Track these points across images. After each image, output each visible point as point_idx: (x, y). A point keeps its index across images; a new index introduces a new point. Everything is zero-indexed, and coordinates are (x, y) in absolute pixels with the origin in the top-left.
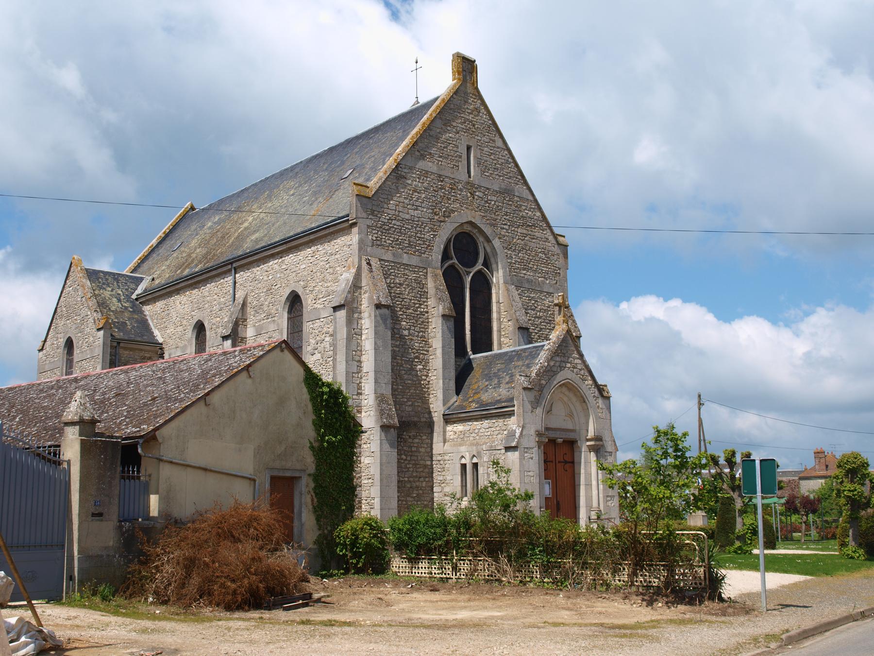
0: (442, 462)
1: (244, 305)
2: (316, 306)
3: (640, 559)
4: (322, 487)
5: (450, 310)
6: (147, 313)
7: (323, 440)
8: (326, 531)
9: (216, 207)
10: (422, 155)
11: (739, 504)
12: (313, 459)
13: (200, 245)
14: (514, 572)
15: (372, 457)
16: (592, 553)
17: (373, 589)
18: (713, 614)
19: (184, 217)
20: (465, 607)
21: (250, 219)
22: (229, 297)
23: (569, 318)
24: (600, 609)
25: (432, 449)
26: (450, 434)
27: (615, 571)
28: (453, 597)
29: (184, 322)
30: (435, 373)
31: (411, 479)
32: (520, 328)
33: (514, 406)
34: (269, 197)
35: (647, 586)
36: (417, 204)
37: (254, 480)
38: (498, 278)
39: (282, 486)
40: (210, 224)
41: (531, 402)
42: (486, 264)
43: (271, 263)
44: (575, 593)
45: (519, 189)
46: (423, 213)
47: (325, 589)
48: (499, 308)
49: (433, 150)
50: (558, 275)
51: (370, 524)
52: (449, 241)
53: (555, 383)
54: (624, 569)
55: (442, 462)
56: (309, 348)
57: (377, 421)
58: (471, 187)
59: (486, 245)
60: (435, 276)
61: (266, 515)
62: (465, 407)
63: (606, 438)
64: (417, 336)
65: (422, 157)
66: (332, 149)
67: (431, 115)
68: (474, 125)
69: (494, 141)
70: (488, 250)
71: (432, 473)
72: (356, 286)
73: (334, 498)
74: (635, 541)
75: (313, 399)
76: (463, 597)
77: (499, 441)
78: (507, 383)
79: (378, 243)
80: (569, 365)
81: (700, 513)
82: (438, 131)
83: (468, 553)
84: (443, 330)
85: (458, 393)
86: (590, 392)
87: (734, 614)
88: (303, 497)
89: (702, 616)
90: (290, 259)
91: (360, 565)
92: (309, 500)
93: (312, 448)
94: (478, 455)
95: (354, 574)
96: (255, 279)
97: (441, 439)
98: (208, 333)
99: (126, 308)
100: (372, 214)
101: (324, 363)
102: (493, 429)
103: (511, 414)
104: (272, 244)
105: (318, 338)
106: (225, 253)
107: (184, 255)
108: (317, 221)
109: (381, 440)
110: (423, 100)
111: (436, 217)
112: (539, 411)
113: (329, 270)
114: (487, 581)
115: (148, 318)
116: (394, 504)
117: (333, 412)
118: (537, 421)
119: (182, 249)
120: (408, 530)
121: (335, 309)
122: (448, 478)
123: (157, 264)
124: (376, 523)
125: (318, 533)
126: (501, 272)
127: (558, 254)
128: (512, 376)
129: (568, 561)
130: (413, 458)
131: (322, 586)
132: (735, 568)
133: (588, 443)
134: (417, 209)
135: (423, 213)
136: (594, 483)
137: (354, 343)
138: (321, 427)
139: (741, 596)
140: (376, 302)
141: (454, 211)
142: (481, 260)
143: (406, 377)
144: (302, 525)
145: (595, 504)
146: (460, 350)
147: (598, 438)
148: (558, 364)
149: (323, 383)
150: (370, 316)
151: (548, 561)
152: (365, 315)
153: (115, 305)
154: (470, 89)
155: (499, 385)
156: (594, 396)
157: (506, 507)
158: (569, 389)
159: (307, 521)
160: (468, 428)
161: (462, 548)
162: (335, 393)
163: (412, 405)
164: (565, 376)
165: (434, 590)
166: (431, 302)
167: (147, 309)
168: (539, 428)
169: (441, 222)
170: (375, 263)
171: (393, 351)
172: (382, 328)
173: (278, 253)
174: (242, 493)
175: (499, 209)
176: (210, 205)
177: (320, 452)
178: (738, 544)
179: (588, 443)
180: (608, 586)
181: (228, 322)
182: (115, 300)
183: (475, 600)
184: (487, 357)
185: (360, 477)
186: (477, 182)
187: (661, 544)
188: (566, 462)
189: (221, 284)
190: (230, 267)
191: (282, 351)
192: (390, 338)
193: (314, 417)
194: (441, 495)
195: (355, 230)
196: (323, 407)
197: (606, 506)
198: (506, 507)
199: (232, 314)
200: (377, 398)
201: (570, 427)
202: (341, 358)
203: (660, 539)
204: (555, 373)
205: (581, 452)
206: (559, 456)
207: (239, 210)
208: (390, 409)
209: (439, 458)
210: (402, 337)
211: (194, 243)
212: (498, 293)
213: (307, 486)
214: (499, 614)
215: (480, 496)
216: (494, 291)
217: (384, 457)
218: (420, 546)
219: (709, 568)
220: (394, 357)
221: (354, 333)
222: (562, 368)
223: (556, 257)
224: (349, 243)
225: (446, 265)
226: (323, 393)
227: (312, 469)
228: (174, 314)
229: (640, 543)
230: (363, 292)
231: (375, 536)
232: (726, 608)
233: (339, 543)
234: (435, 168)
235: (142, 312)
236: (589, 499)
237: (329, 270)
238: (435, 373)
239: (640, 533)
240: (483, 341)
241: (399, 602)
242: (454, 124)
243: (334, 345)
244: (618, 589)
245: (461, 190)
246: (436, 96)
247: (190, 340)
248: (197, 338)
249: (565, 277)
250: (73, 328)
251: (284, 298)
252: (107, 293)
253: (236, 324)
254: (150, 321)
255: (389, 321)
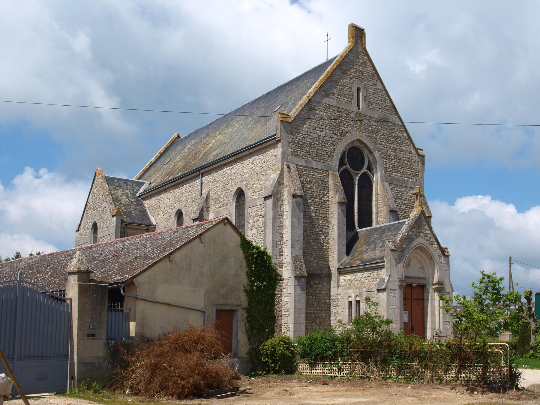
0: (336, 300)
1: (207, 198)
2: (254, 197)
3: (464, 362)
4: (252, 317)
5: (343, 198)
6: (146, 205)
7: (253, 285)
8: (255, 346)
9: (192, 136)
10: (326, 94)
11: (533, 326)
12: (246, 298)
13: (181, 160)
14: (379, 372)
15: (288, 298)
16: (431, 358)
17: (283, 384)
18: (511, 399)
19: (173, 143)
20: (343, 396)
21: (214, 141)
22: (198, 193)
23: (424, 203)
24: (434, 396)
25: (330, 291)
26: (342, 282)
27: (446, 371)
28: (336, 388)
29: (170, 211)
30: (333, 241)
31: (316, 312)
32: (391, 211)
33: (384, 262)
34: (227, 127)
35: (468, 380)
36: (323, 127)
37: (205, 312)
38: (377, 178)
39: (224, 316)
40: (189, 146)
41: (396, 259)
42: (369, 168)
43: (225, 169)
44: (419, 385)
45: (393, 118)
46: (326, 134)
47: (250, 384)
48: (377, 198)
49: (334, 91)
50: (418, 176)
51: (286, 342)
52: (344, 153)
53: (412, 246)
54: (452, 369)
55: (336, 300)
56: (249, 226)
57: (292, 273)
58: (360, 117)
59: (369, 155)
60: (334, 176)
61: (211, 334)
62: (352, 264)
63: (446, 283)
64: (321, 217)
65: (327, 95)
66: (268, 94)
67: (333, 66)
68: (362, 74)
69: (376, 85)
70: (371, 159)
71: (330, 307)
72: (280, 183)
73: (261, 324)
74: (460, 350)
75: (246, 258)
76: (343, 388)
77: (374, 286)
78: (381, 247)
79: (296, 153)
80: (422, 235)
81: (508, 333)
82: (338, 77)
83: (348, 359)
84: (338, 212)
85: (348, 254)
86: (434, 249)
87: (526, 399)
88: (239, 323)
89: (504, 400)
90: (237, 166)
91: (277, 368)
92: (243, 324)
93: (245, 290)
94: (360, 295)
95: (273, 374)
96: (215, 181)
97: (336, 285)
98: (184, 217)
99: (132, 202)
100: (292, 134)
101: (259, 235)
102: (370, 278)
103: (382, 267)
104: (225, 156)
105: (255, 219)
106: (196, 164)
107: (171, 167)
108: (255, 140)
109: (295, 286)
110: (330, 58)
111: (335, 136)
112: (401, 265)
113: (262, 172)
114: (360, 378)
115: (147, 208)
116: (303, 328)
117: (261, 268)
118: (399, 272)
119: (170, 163)
120: (309, 344)
121: (266, 198)
122: (340, 310)
123: (154, 173)
124: (288, 340)
125: (249, 347)
126: (379, 173)
127: (418, 162)
128: (384, 242)
129: (415, 364)
130: (317, 298)
131: (249, 382)
132: (529, 368)
133: (434, 287)
134: (322, 131)
135: (326, 134)
136: (437, 313)
137: (278, 221)
138: (252, 276)
139: (531, 386)
140: (293, 193)
141: (348, 132)
142: (366, 166)
143: (313, 244)
144: (238, 342)
145: (437, 327)
146: (350, 226)
147: (440, 283)
148: (414, 234)
149: (254, 247)
150: (289, 203)
151: (402, 365)
152: (286, 202)
153: (124, 200)
154: (360, 49)
155: (375, 249)
156: (439, 255)
157: (374, 329)
158: (422, 251)
159: (241, 339)
160: (354, 277)
161: (344, 356)
162: (263, 254)
163: (317, 263)
164: (419, 242)
165: (325, 384)
166: (331, 194)
167: (146, 203)
168: (401, 276)
169: (339, 139)
170: (293, 167)
171: (305, 227)
172: (297, 211)
173: (230, 163)
174: (196, 321)
175: (378, 131)
176: (190, 135)
177: (250, 293)
178: (531, 352)
179: (434, 287)
180: (441, 380)
181: (197, 209)
182: (124, 197)
183: (350, 390)
184: (368, 230)
185: (281, 311)
186: (364, 113)
187: (478, 352)
188: (418, 299)
189: (193, 185)
190: (198, 173)
191: (225, 225)
192: (302, 218)
193: (247, 270)
194: (335, 322)
195: (280, 145)
196: (253, 263)
197: (445, 328)
198: (374, 329)
199: (199, 204)
200: (292, 258)
201: (422, 275)
202: (269, 231)
203: (477, 349)
204: (413, 240)
205: (428, 292)
206: (414, 295)
207: (207, 135)
208: (302, 265)
209: (335, 297)
210: (311, 217)
211: (178, 159)
212: (376, 188)
213: (242, 316)
214: (365, 400)
215: (358, 322)
216: (374, 187)
217: (297, 297)
218: (317, 355)
219: (511, 367)
220: (305, 230)
221: (278, 215)
222: (417, 236)
223: (416, 163)
224: (276, 154)
225: (342, 169)
226: (253, 253)
227: (245, 304)
228: (163, 206)
229: (464, 352)
230: (284, 186)
231: (288, 349)
232: (521, 395)
233: (263, 354)
234: (335, 103)
235: (142, 205)
236: (433, 323)
237: (262, 172)
238: (333, 241)
239: (464, 345)
240: (366, 219)
241: (299, 392)
242: (349, 73)
243: (265, 223)
244: (448, 383)
245: (353, 118)
246: (337, 55)
247: (173, 223)
248: (178, 221)
249: (422, 177)
250: (98, 215)
251: (233, 193)
252: (119, 193)
253: (202, 211)
254: (148, 211)
255: (302, 206)
